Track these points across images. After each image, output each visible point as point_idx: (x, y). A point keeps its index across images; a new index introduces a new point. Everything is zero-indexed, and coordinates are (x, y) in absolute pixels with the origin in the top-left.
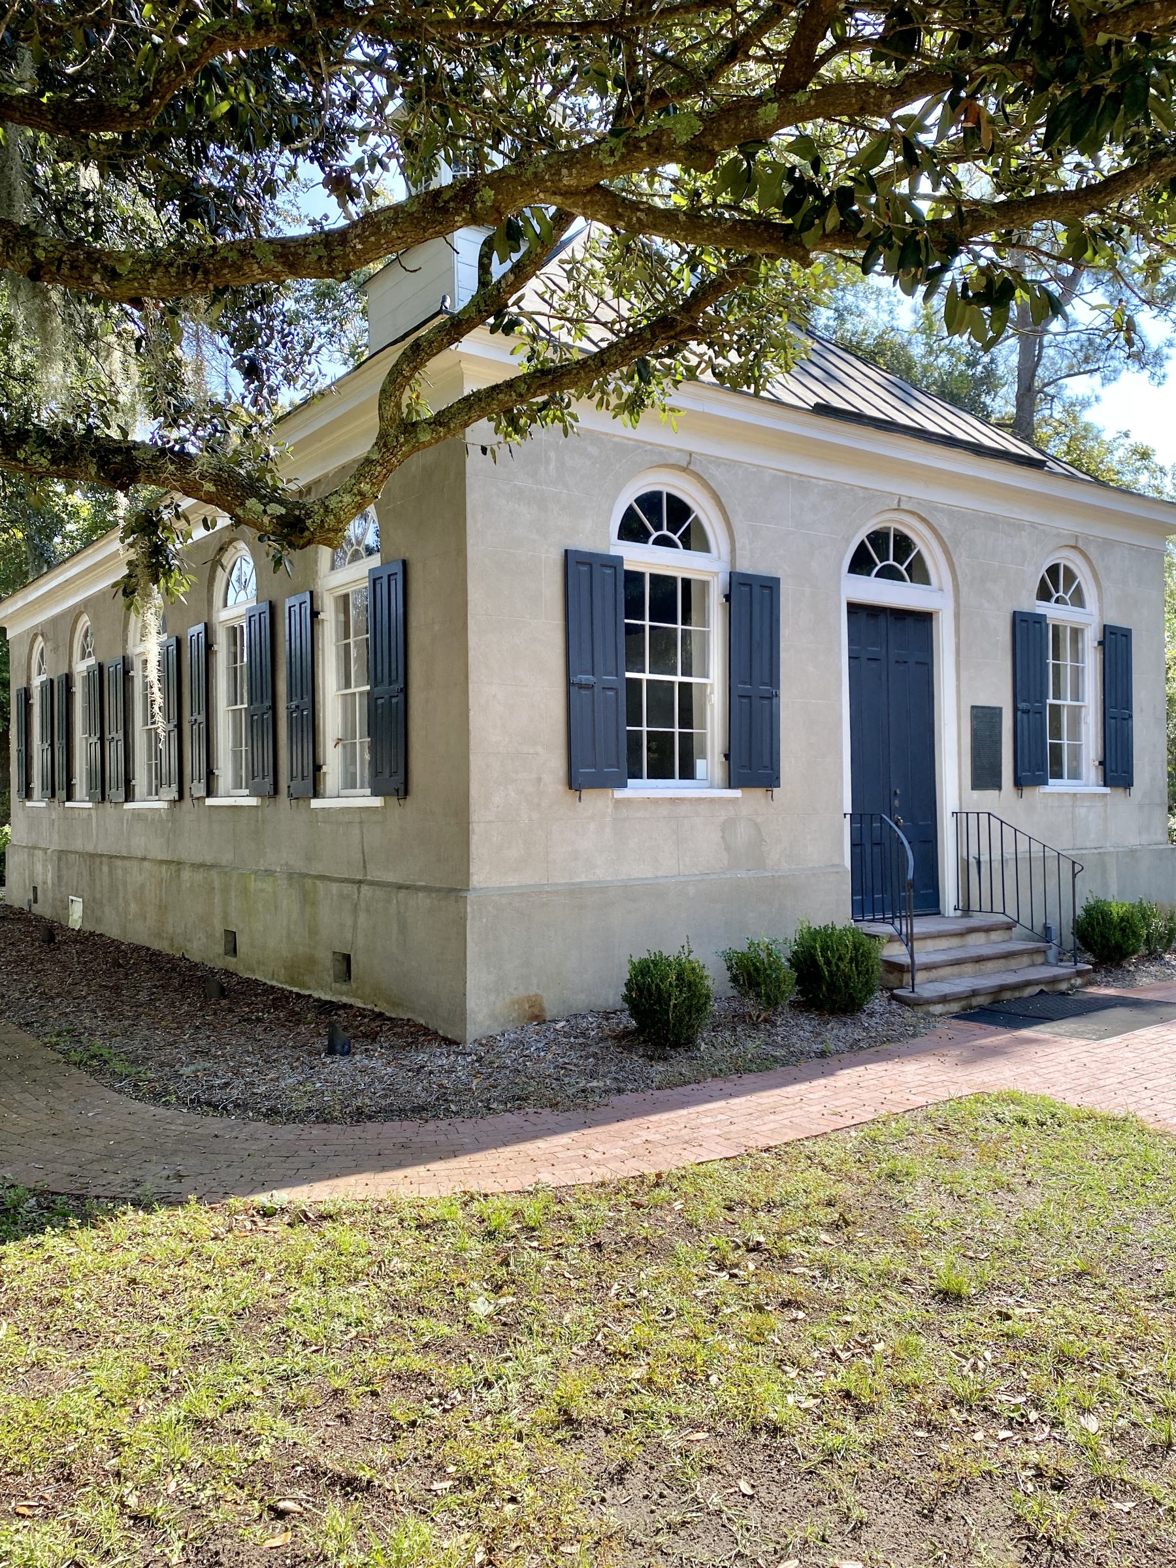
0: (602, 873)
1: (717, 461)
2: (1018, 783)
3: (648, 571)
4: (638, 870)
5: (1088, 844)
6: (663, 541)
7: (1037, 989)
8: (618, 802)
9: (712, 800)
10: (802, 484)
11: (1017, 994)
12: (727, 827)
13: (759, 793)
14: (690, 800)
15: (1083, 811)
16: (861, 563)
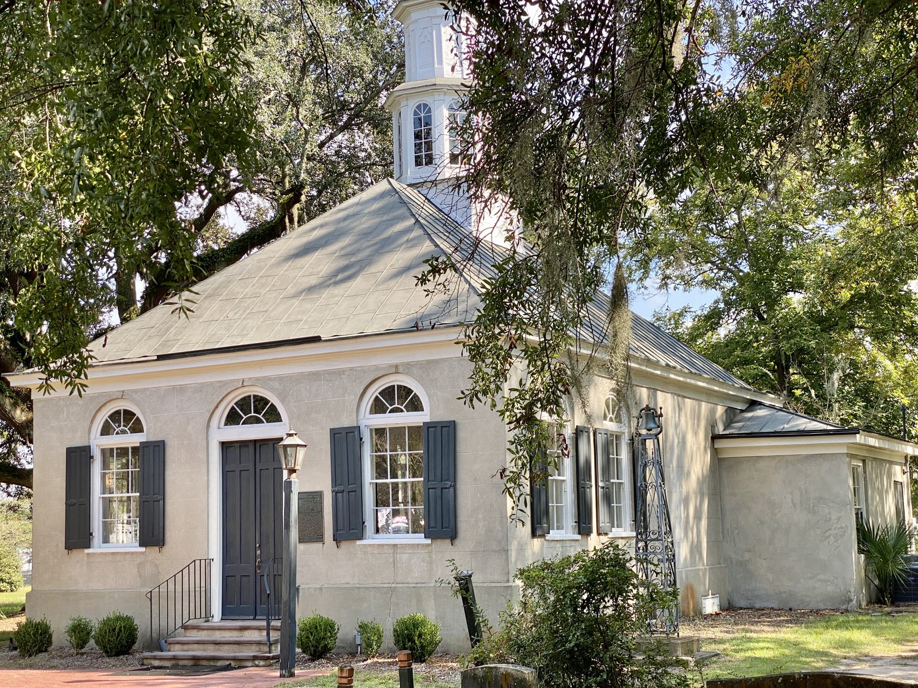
0: (81, 586)
1: (136, 391)
2: (337, 539)
3: (130, 446)
4: (96, 586)
5: (410, 580)
6: (124, 432)
7: (227, 663)
8: (88, 554)
9: (132, 553)
10: (182, 389)
11: (212, 663)
12: (140, 566)
13: (157, 548)
14: (121, 553)
15: (405, 557)
16: (233, 418)
